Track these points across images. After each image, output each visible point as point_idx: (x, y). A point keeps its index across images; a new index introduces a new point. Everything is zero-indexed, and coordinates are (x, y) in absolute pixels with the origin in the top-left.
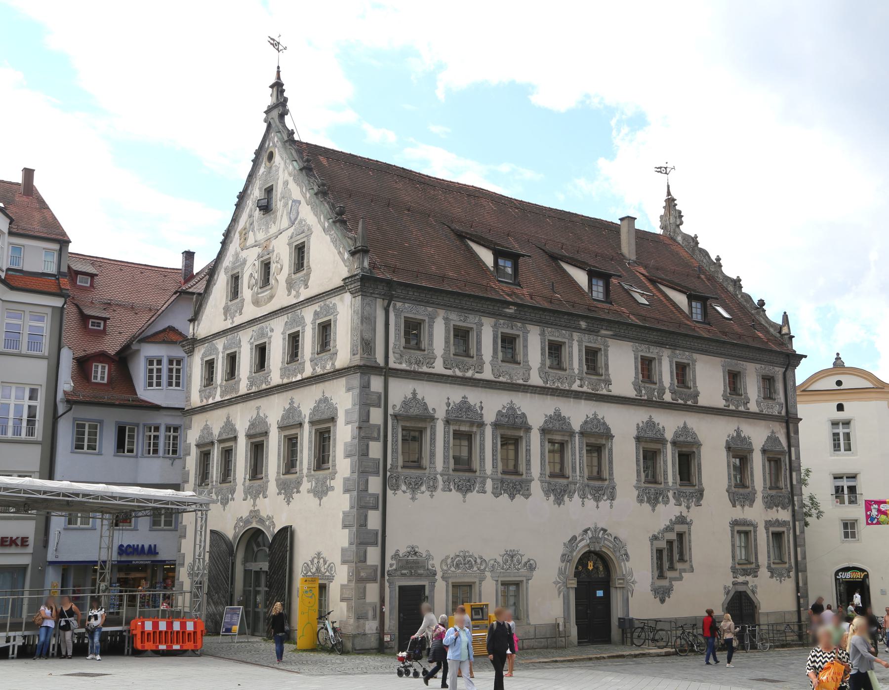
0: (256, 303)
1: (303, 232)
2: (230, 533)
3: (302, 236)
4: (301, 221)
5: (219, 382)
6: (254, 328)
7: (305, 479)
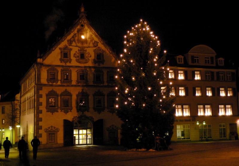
0: (78, 61)
1: (100, 50)
2: (71, 120)
4: (99, 47)
5: (59, 78)
6: (79, 69)
7: (106, 109)
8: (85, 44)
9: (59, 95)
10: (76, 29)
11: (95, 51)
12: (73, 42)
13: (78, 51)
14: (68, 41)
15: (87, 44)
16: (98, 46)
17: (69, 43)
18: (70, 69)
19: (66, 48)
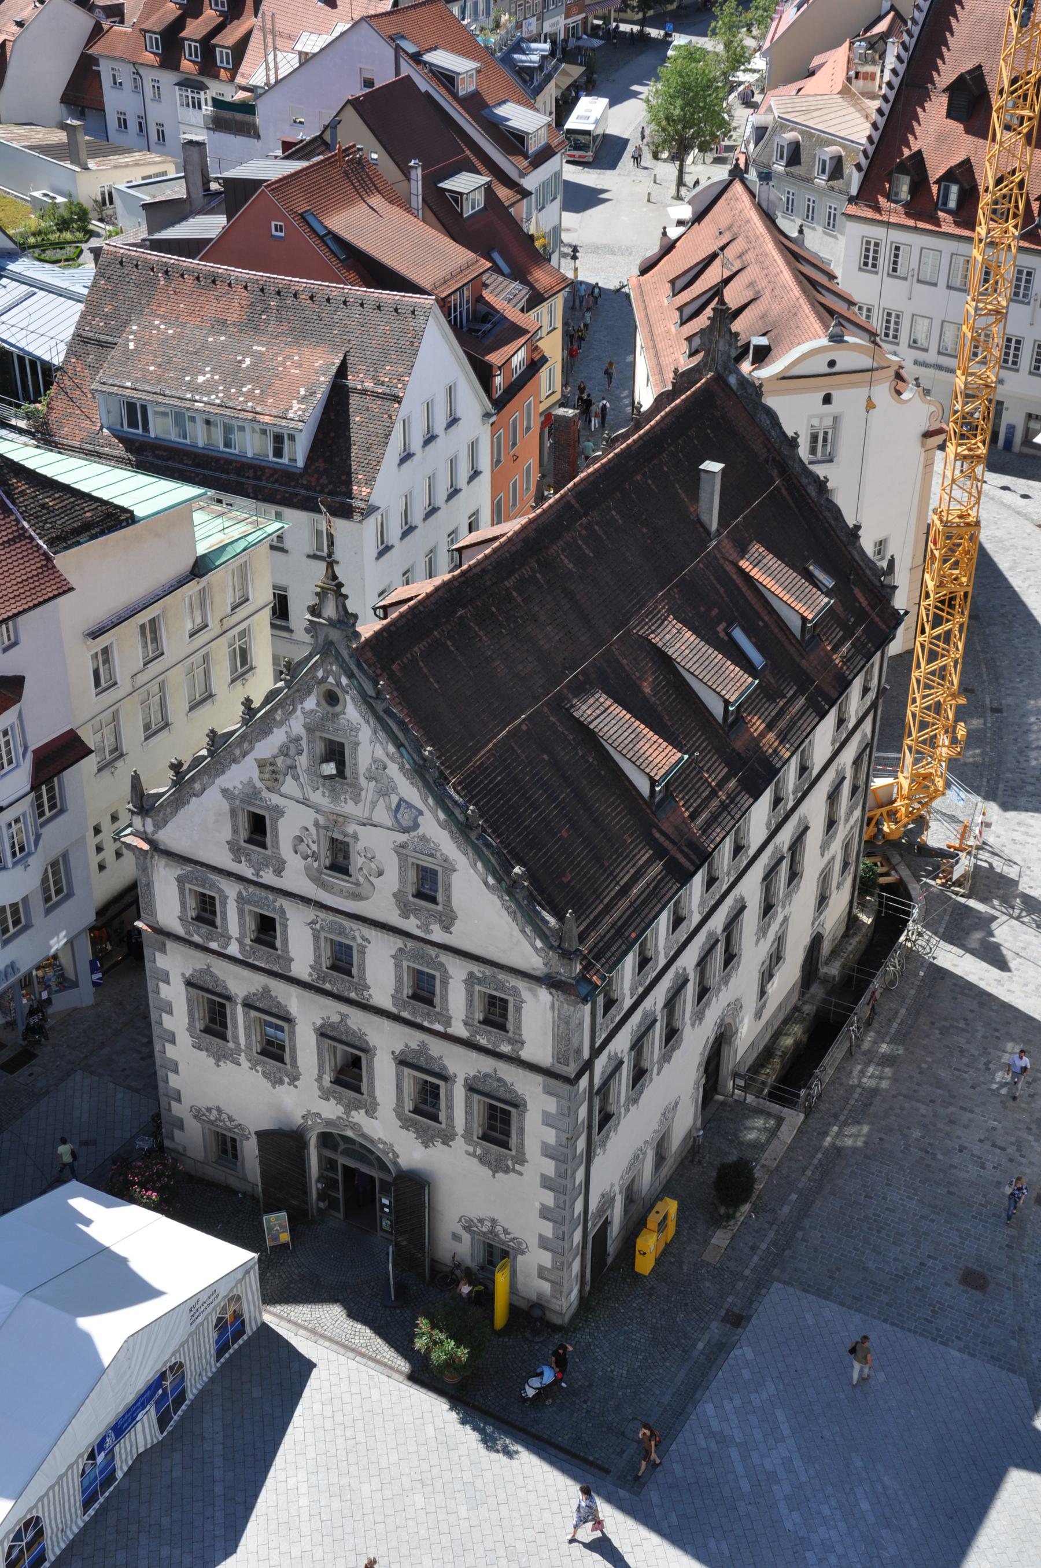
1: (432, 855)
3: (430, 859)
4: (424, 839)
8: (350, 802)
9: (239, 1001)
10: (299, 712)
11: (404, 851)
12: (289, 778)
13: (313, 830)
14: (261, 764)
15: (361, 804)
16: (420, 831)
17: (267, 776)
18: (278, 904)
19: (252, 794)
